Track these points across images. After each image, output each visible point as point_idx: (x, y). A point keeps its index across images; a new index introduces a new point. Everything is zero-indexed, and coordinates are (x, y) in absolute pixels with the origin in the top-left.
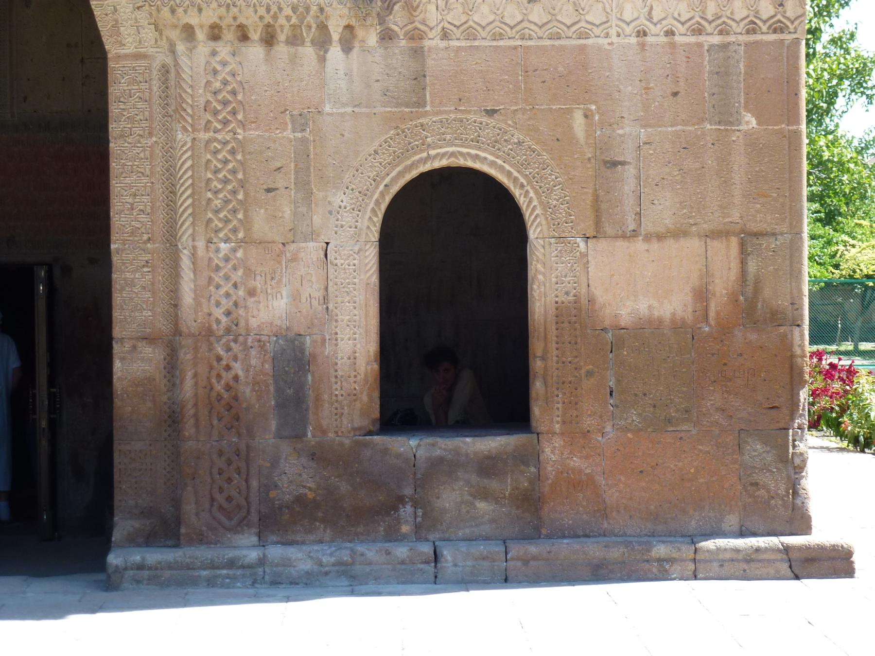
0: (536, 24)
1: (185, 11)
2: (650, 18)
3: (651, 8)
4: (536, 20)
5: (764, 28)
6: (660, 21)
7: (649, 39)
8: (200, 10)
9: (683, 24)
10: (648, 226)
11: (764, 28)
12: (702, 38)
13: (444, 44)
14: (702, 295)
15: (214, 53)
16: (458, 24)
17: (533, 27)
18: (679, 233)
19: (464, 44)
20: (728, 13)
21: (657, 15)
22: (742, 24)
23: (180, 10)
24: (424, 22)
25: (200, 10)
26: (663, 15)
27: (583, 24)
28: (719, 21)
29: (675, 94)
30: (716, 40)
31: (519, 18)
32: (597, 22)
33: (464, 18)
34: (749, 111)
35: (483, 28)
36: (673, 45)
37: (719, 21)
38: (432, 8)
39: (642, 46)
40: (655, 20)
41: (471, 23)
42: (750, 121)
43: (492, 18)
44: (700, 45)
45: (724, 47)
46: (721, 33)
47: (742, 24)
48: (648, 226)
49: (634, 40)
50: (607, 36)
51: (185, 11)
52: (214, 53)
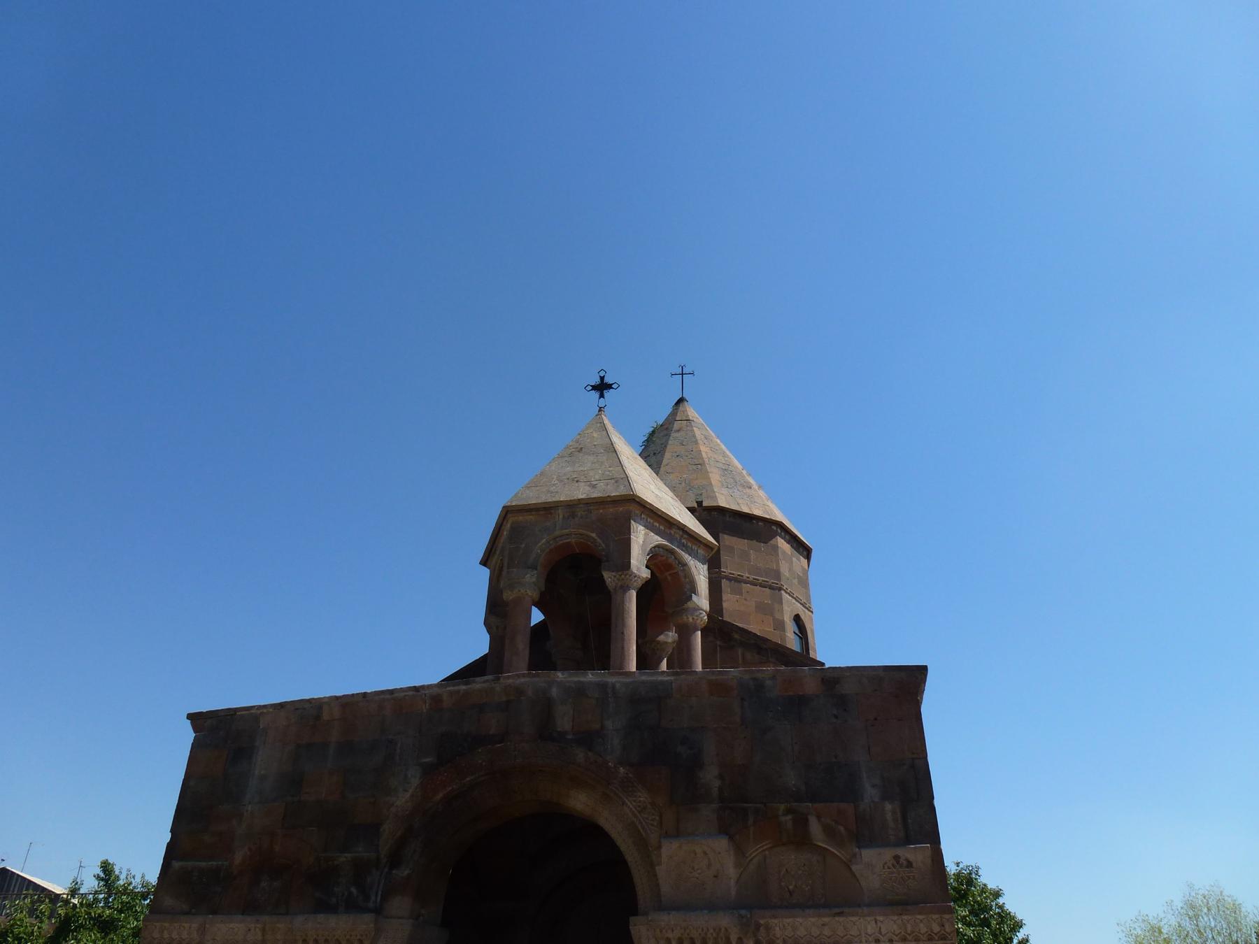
0: (826, 936)
1: (666, 931)
3: (880, 928)
4: (826, 934)
5: (937, 938)
6: (885, 934)
8: (673, 931)
9: (897, 936)
11: (937, 938)
16: (790, 936)
17: (824, 937)
20: (917, 930)
21: (883, 931)
22: (925, 936)
23: (664, 931)
25: (673, 931)
26: (886, 932)
27: (849, 936)
28: (914, 934)
31: (818, 933)
32: (856, 935)
33: (792, 934)
35: (802, 938)
37: (914, 934)
38: (778, 929)
40: (883, 933)
41: (796, 936)
43: (806, 933)
47: (925, 936)
51: (666, 931)
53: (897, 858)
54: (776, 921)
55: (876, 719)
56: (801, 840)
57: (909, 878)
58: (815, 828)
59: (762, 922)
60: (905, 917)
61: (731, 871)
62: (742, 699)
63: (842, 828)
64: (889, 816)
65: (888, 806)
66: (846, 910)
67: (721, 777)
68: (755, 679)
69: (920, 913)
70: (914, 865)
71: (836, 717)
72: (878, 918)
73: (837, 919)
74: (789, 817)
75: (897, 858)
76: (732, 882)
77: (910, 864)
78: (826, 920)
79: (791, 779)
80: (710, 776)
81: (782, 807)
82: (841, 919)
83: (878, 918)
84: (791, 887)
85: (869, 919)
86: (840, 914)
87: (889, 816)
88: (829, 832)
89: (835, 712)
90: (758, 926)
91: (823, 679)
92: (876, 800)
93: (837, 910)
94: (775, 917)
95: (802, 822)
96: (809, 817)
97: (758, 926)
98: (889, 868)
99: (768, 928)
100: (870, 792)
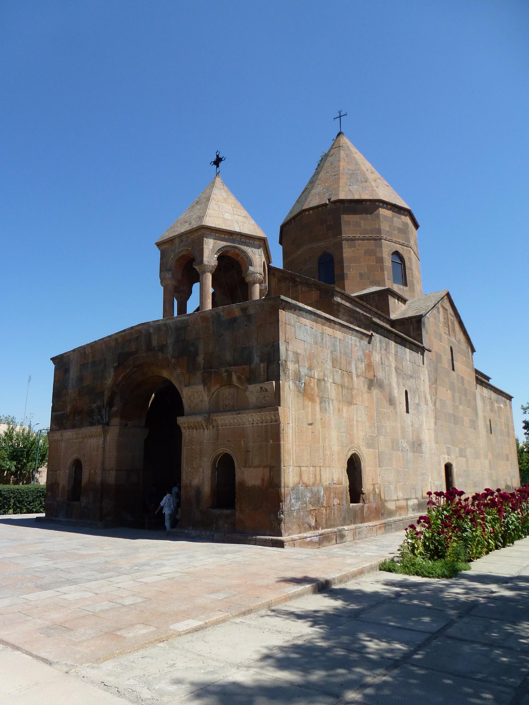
2: (253, 421)
7: (254, 425)
10: (254, 465)
12: (263, 424)
13: (221, 428)
14: (263, 480)
15: (189, 432)
18: (259, 466)
19: (225, 427)
24: (218, 424)
29: (258, 436)
30: (265, 424)
34: (272, 439)
36: (258, 426)
39: (253, 426)
42: (271, 442)
44: (262, 426)
45: (266, 426)
46: (266, 423)
48: (254, 465)
49: (251, 425)
50: (247, 424)
52: (189, 432)
53: (261, 388)
54: (218, 418)
55: (261, 325)
56: (230, 384)
57: (266, 396)
58: (234, 378)
59: (214, 418)
60: (262, 413)
61: (206, 399)
62: (213, 323)
63: (243, 377)
64: (262, 369)
65: (262, 365)
66: (241, 411)
67: (204, 359)
68: (216, 313)
69: (267, 411)
70: (268, 390)
71: (246, 326)
72: (252, 414)
73: (238, 415)
74: (225, 374)
75: (261, 388)
76: (207, 403)
77: (266, 390)
78: (235, 416)
79: (228, 356)
80: (201, 359)
81: (224, 369)
82: (240, 415)
83: (252, 414)
84: (227, 403)
85: (249, 415)
86: (239, 413)
87: (262, 369)
88: (239, 378)
89: (246, 323)
90: (213, 420)
91: (241, 309)
92: (258, 362)
93: (238, 412)
94: (217, 416)
95: (230, 375)
96: (232, 373)
97: (213, 420)
98: (259, 393)
99: (216, 421)
100: (256, 359)
